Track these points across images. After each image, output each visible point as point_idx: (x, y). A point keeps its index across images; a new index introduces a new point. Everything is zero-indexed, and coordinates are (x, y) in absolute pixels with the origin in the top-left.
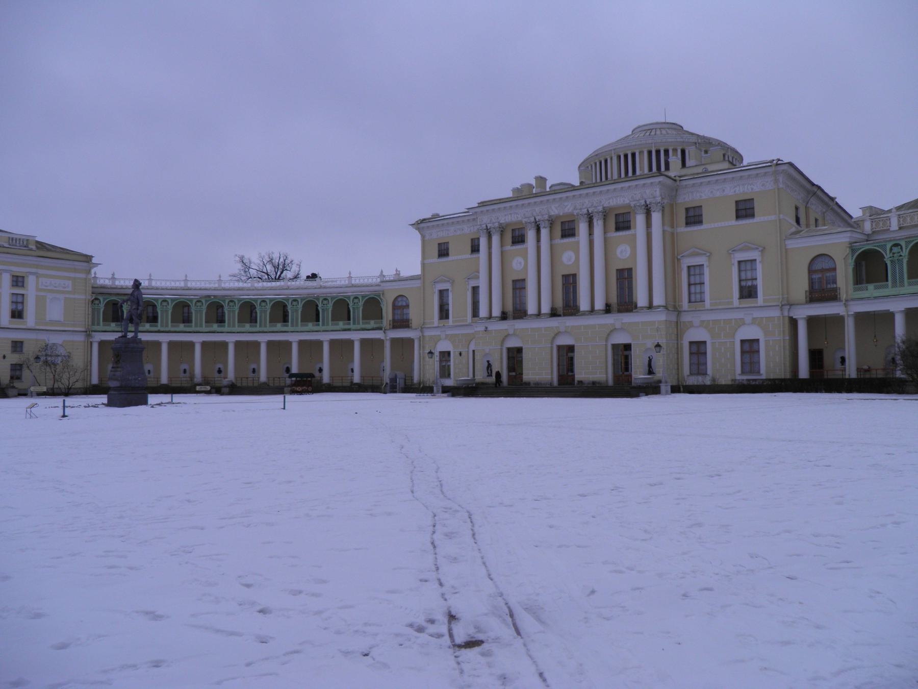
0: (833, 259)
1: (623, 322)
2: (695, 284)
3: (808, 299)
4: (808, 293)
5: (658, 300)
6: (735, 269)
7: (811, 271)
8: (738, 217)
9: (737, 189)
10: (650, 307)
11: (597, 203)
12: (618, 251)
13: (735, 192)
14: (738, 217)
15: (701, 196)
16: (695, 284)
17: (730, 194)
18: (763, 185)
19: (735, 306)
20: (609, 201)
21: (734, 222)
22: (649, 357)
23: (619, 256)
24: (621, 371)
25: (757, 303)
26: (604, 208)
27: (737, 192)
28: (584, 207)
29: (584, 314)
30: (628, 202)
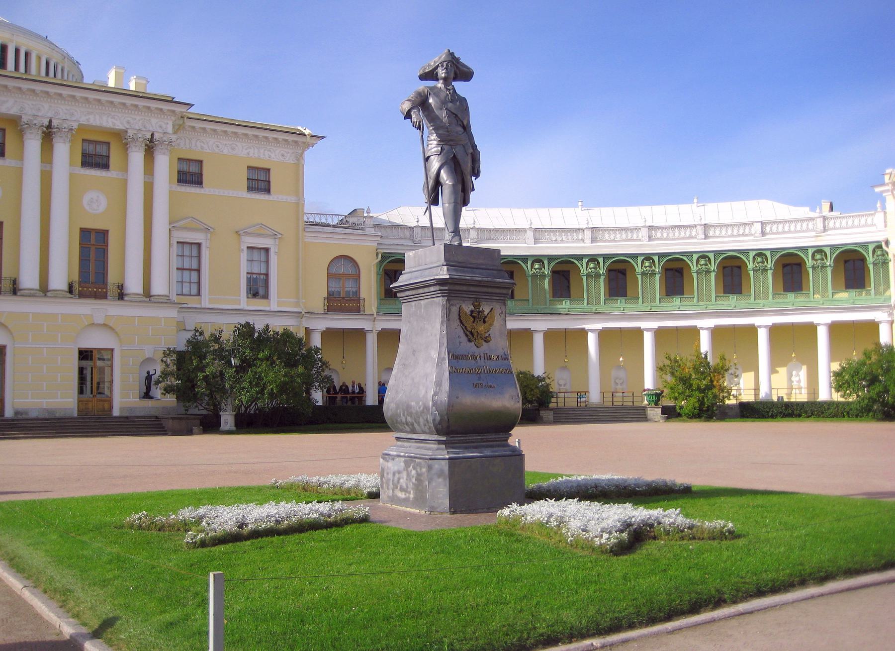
0: (358, 266)
1: (109, 314)
2: (191, 270)
3: (326, 308)
4: (326, 300)
5: (159, 287)
6: (244, 256)
7: (330, 276)
8: (250, 189)
9: (251, 151)
10: (147, 293)
11: (66, 114)
12: (86, 199)
13: (249, 154)
14: (250, 189)
15: (202, 148)
16: (191, 270)
17: (241, 155)
18: (283, 155)
19: (241, 307)
20: (87, 117)
21: (245, 194)
22: (148, 373)
23: (87, 207)
24: (92, 393)
25: (269, 306)
26: (80, 125)
27: (251, 154)
28: (74, 119)
29: (31, 294)
30: (121, 127)
